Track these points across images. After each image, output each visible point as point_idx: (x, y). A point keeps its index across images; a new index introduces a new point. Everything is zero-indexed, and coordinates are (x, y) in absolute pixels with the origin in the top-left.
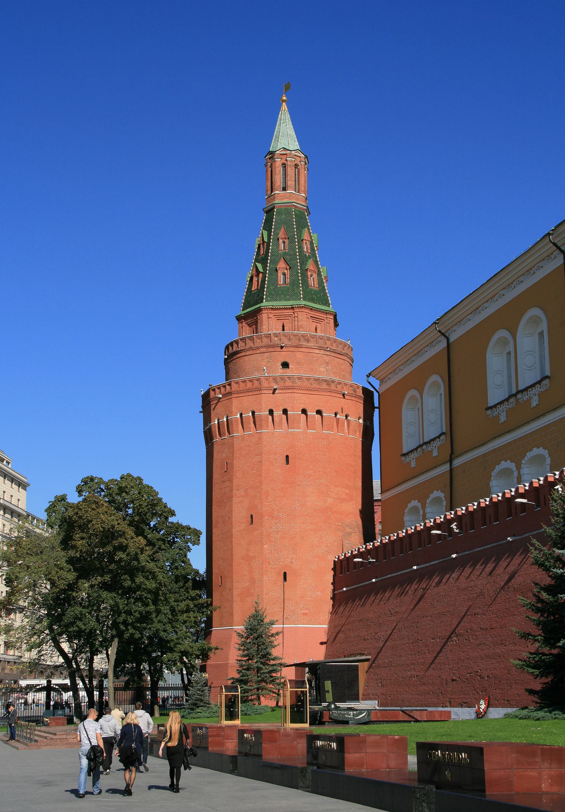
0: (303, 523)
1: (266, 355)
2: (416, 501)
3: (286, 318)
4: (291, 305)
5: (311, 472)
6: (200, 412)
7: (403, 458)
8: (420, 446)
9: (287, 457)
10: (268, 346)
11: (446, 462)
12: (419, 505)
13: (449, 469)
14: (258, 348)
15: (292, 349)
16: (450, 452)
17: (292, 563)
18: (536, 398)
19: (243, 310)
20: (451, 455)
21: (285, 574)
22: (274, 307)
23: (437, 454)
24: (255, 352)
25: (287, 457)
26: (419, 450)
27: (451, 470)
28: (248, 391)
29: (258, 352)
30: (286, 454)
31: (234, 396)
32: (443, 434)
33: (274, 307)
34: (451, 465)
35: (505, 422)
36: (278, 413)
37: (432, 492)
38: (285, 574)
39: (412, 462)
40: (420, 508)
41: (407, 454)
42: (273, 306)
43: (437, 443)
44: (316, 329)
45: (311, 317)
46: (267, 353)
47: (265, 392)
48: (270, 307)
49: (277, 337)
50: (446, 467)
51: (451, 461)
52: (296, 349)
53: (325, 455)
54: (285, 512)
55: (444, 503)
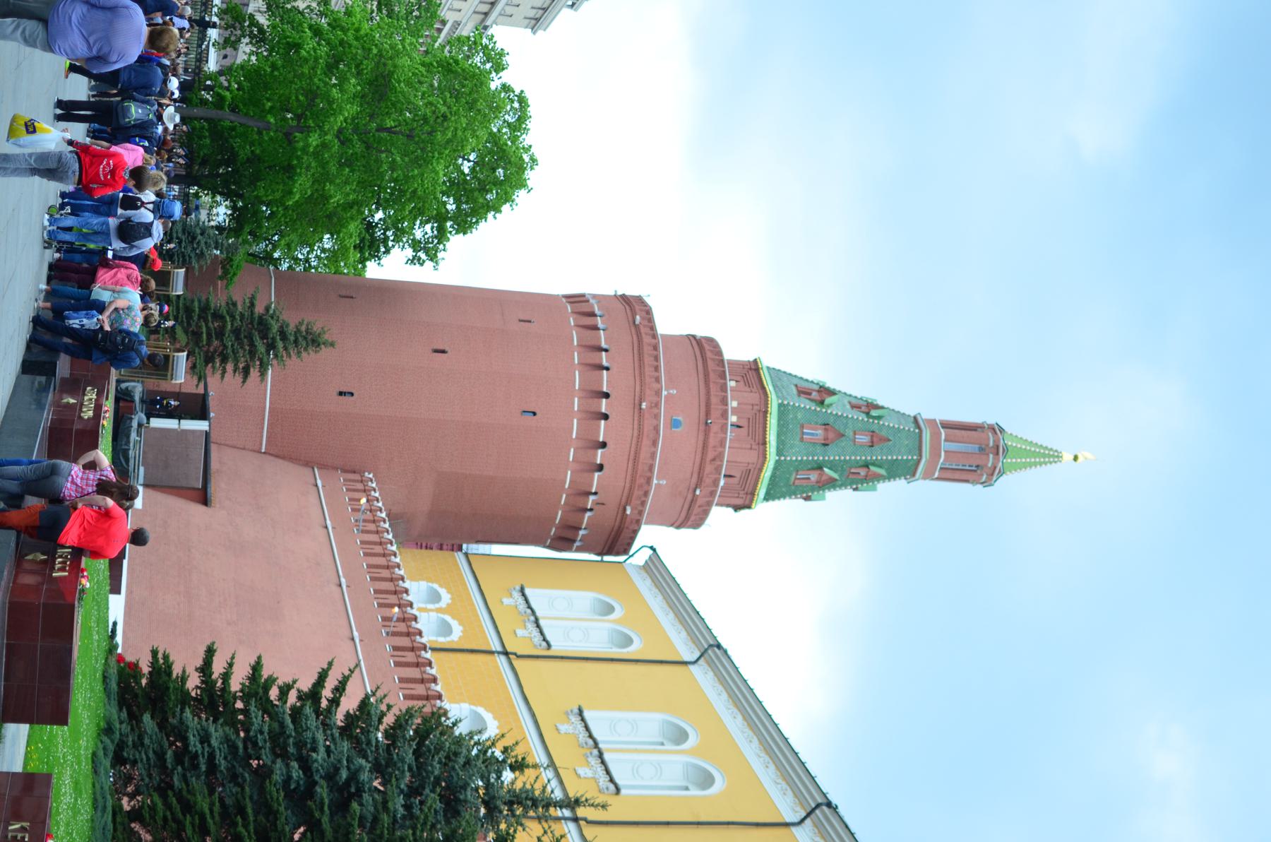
2: (450, 601)
7: (518, 588)
8: (533, 612)
11: (503, 645)
12: (443, 604)
13: (494, 649)
16: (519, 653)
18: (590, 774)
19: (768, 368)
20: (515, 654)
26: (529, 611)
27: (492, 653)
30: (538, 412)
32: (549, 646)
34: (499, 653)
36: (604, 405)
37: (460, 624)
39: (511, 600)
40: (437, 606)
41: (524, 595)
43: (537, 638)
44: (731, 476)
45: (750, 470)
51: (506, 653)
55: (441, 639)
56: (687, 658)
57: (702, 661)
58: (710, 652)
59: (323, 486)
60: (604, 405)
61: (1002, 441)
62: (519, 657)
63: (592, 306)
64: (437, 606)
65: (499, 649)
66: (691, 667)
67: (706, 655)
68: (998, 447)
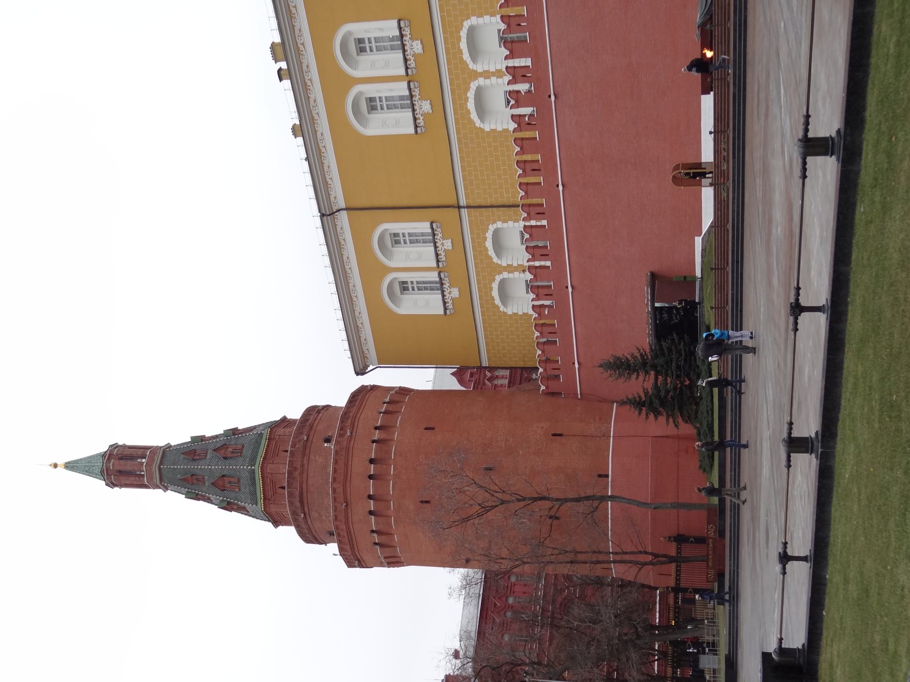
1: (312, 457)
3: (278, 447)
4: (266, 439)
7: (448, 312)
9: (426, 429)
12: (498, 278)
13: (466, 209)
14: (302, 466)
15: (312, 432)
21: (554, 435)
25: (426, 429)
27: (468, 207)
28: (346, 465)
29: (306, 467)
30: (423, 429)
33: (263, 456)
34: (464, 207)
35: (431, 104)
36: (377, 435)
38: (554, 435)
42: (261, 457)
47: (352, 445)
48: (262, 459)
49: (295, 445)
50: (464, 212)
51: (459, 207)
52: (314, 428)
60: (377, 435)
61: (104, 463)
64: (501, 277)
65: (462, 210)
66: (344, 207)
68: (108, 459)
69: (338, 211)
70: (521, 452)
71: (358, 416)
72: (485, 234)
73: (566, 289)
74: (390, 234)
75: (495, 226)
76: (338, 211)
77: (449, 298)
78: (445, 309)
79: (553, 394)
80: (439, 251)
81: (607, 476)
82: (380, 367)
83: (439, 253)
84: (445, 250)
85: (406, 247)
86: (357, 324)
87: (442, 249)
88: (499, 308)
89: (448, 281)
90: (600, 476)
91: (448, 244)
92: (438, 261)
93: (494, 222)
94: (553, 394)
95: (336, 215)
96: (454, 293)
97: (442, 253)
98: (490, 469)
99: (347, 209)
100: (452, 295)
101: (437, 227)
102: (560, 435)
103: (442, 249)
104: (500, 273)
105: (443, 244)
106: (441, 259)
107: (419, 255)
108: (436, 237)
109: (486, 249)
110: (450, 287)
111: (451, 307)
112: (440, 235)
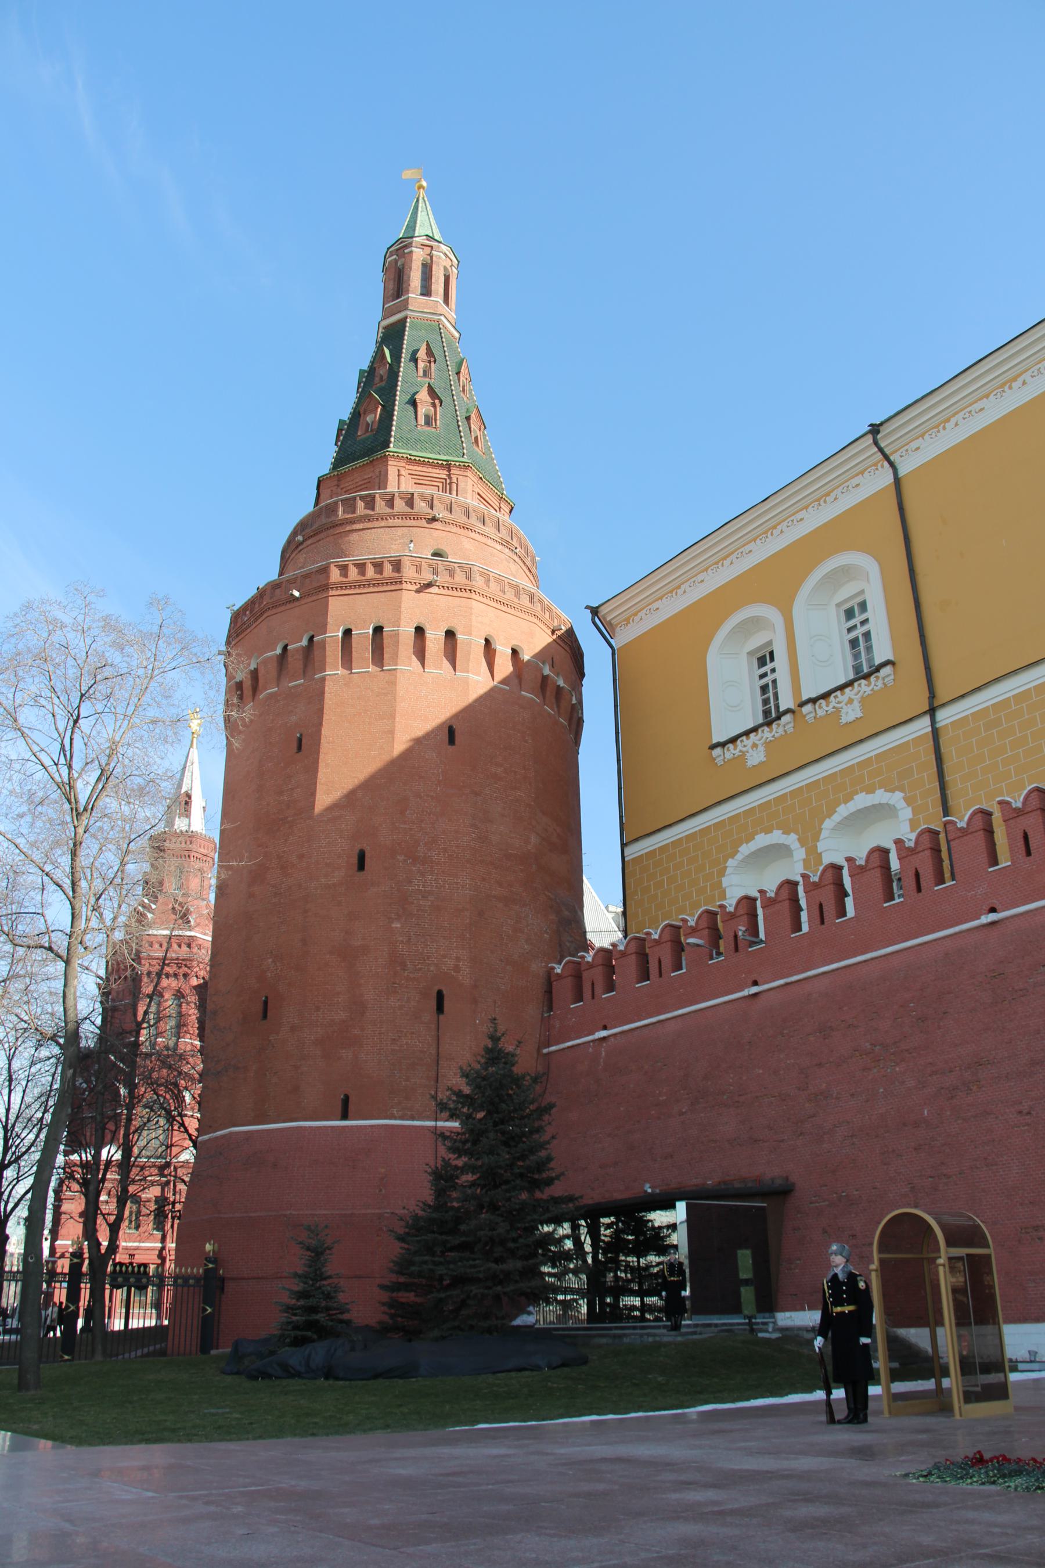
0: (484, 879)
1: (400, 531)
5: (500, 770)
6: (220, 653)
7: (718, 751)
10: (405, 516)
13: (930, 729)
15: (455, 529)
16: (927, 695)
17: (457, 968)
21: (440, 996)
22: (413, 458)
23: (859, 714)
24: (376, 524)
27: (935, 733)
28: (370, 583)
31: (331, 593)
33: (413, 458)
38: (440, 996)
46: (404, 529)
51: (932, 711)
53: (526, 742)
54: (445, 850)
56: (890, 479)
57: (892, 458)
58: (882, 445)
59: (605, 1028)
62: (932, 696)
63: (265, 662)
65: (926, 721)
66: (902, 473)
67: (887, 451)
69: (892, 465)
70: (398, 925)
71: (476, 597)
72: (880, 788)
73: (750, 982)
74: (862, 592)
75: (902, 804)
76: (892, 465)
77: (745, 746)
78: (722, 745)
79: (549, 992)
80: (836, 697)
81: (345, 1116)
82: (613, 654)
83: (832, 698)
84: (838, 711)
85: (840, 631)
86: (683, 584)
87: (839, 703)
88: (733, 858)
89: (777, 735)
90: (346, 1101)
91: (851, 713)
92: (813, 701)
93: (908, 801)
94: (549, 992)
95: (882, 466)
96: (754, 754)
97: (831, 706)
98: (361, 865)
99: (897, 481)
100: (750, 750)
101: (883, 679)
102: (440, 1008)
103: (839, 703)
104: (802, 842)
105: (850, 701)
106: (820, 707)
107: (824, 662)
108: (863, 682)
109: (848, 799)
110: (767, 744)
111: (728, 756)
112: (868, 690)
